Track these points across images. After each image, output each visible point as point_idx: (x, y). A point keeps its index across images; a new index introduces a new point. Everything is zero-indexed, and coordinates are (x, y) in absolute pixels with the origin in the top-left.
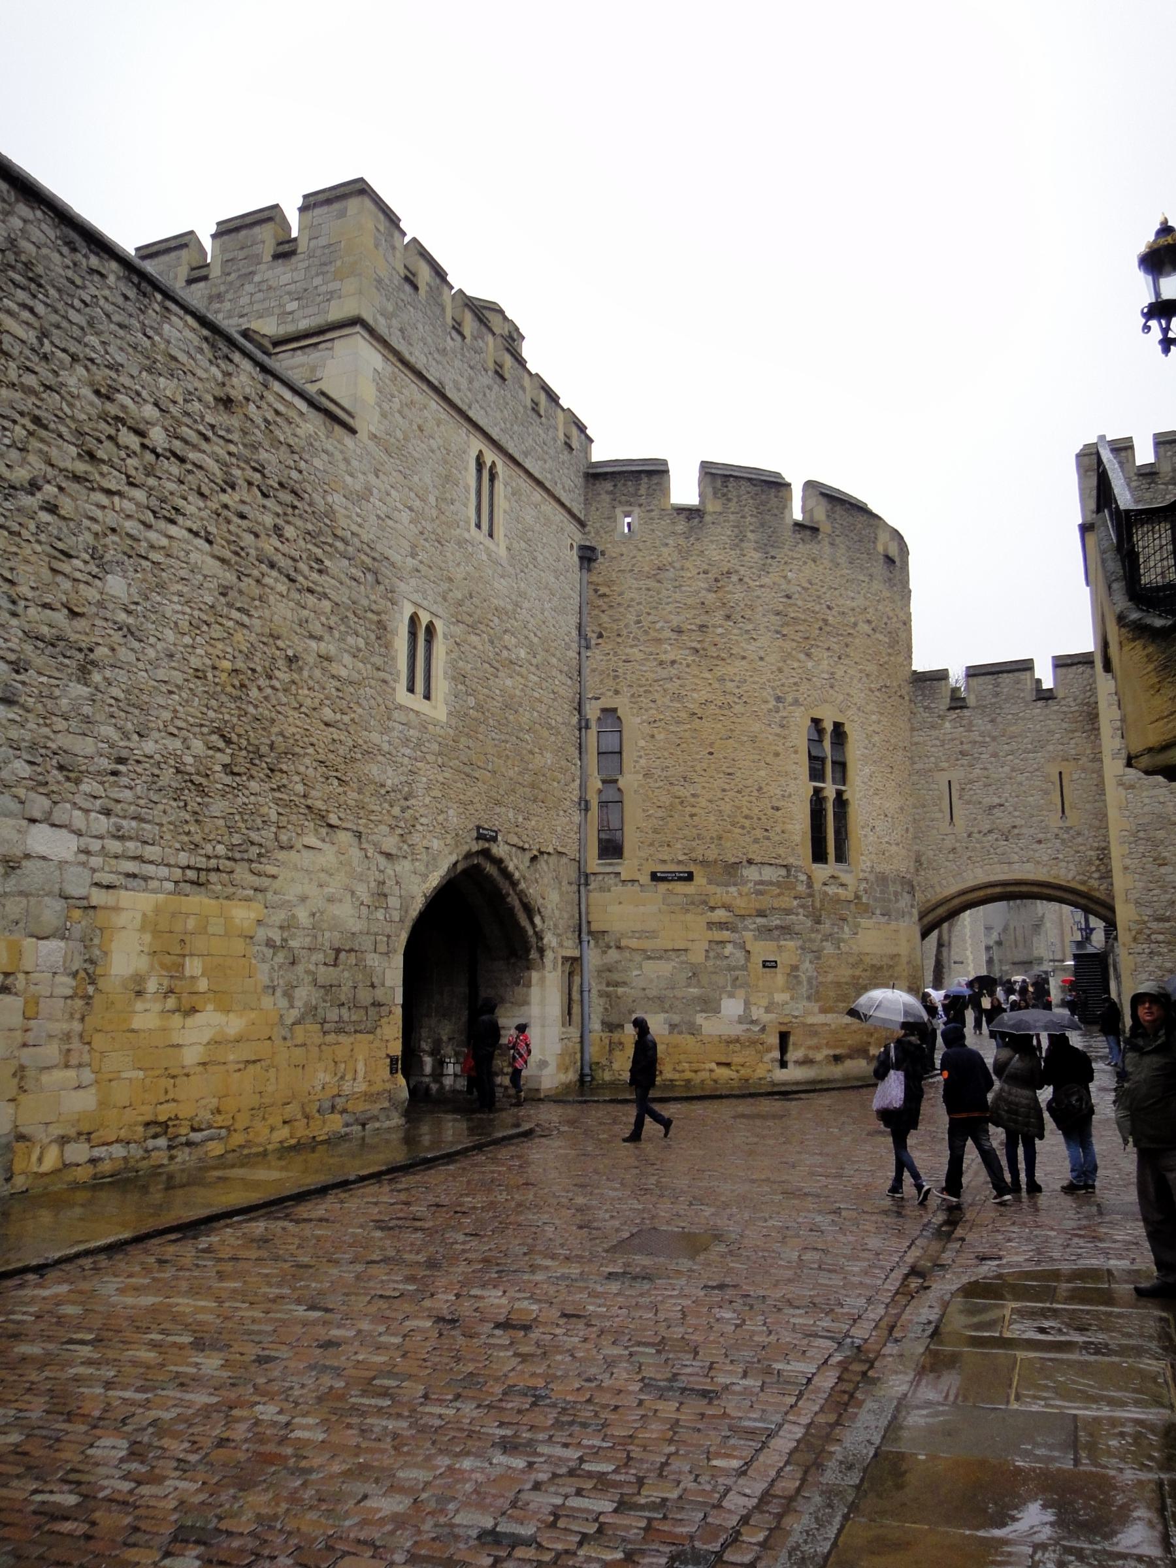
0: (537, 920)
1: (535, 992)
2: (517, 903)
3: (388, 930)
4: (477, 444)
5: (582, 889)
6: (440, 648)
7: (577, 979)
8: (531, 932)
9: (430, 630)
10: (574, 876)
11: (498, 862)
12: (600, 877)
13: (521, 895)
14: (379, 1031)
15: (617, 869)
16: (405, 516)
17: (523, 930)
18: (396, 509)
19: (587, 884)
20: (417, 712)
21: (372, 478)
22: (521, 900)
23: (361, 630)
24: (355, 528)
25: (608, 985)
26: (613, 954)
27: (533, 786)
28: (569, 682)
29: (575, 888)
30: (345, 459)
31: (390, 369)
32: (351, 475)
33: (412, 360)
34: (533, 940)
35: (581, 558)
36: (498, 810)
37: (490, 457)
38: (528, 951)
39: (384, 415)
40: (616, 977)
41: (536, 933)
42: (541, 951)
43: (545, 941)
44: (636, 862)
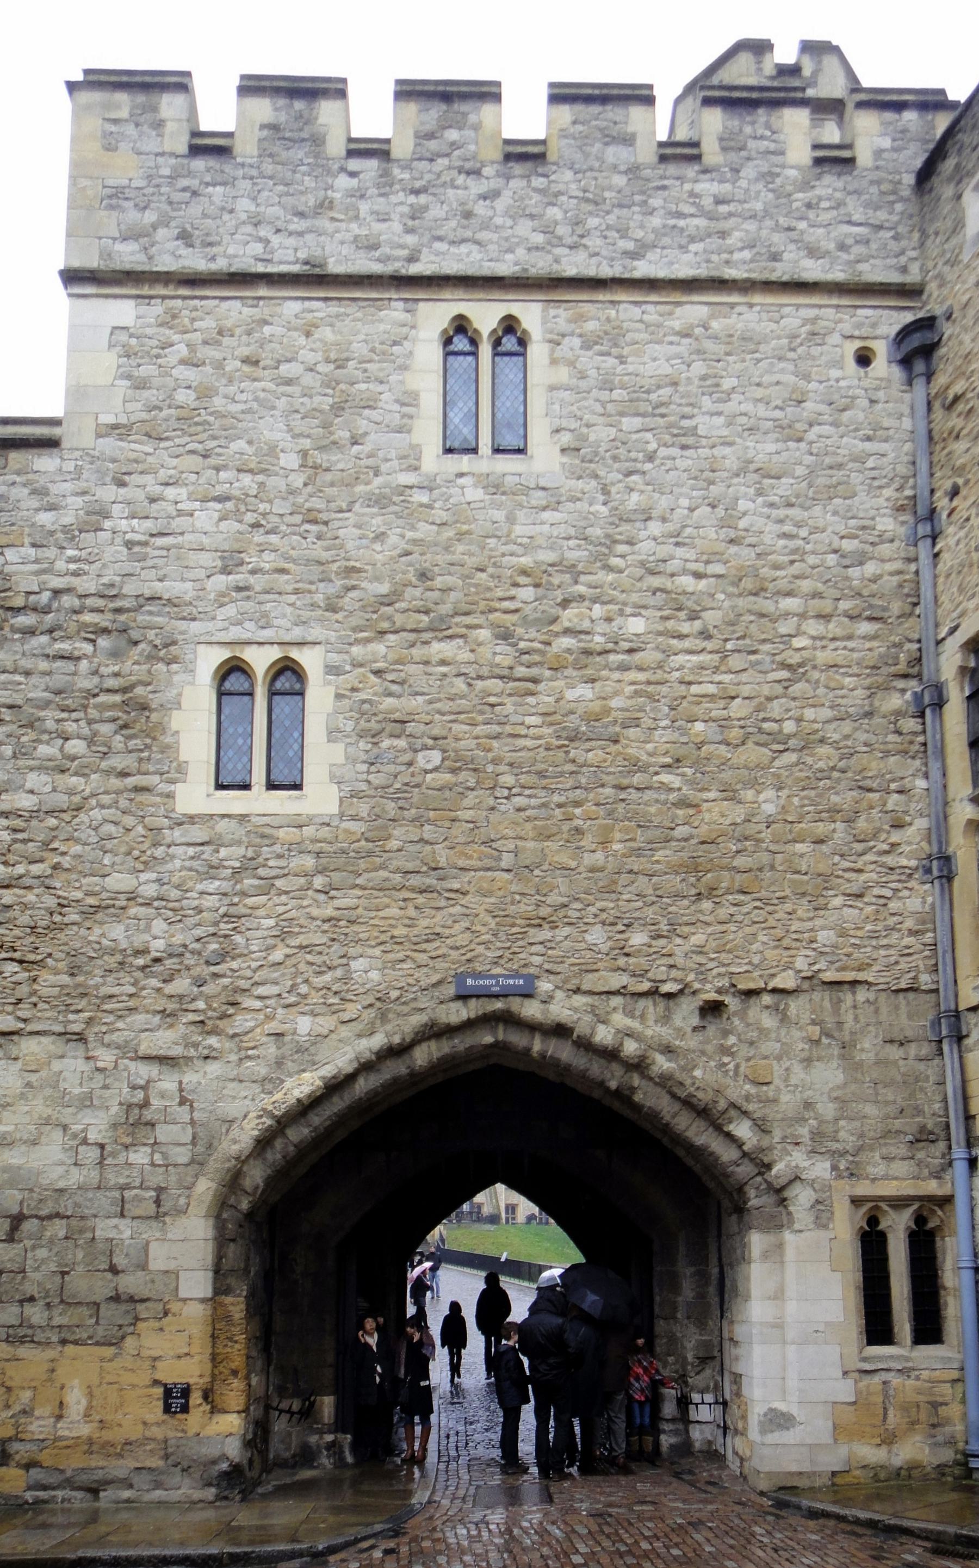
0: (742, 1130)
3: (157, 1179)
4: (437, 314)
6: (319, 698)
8: (727, 1154)
9: (288, 675)
11: (560, 1031)
14: (130, 1342)
16: (206, 517)
17: (699, 1153)
18: (180, 513)
19: (959, 1038)
20: (243, 818)
21: (108, 493)
22: (674, 1096)
23: (71, 727)
24: (57, 583)
27: (694, 867)
28: (865, 628)
30: (34, 492)
31: (157, 309)
32: (52, 508)
33: (221, 265)
35: (906, 362)
37: (485, 315)
39: (141, 385)
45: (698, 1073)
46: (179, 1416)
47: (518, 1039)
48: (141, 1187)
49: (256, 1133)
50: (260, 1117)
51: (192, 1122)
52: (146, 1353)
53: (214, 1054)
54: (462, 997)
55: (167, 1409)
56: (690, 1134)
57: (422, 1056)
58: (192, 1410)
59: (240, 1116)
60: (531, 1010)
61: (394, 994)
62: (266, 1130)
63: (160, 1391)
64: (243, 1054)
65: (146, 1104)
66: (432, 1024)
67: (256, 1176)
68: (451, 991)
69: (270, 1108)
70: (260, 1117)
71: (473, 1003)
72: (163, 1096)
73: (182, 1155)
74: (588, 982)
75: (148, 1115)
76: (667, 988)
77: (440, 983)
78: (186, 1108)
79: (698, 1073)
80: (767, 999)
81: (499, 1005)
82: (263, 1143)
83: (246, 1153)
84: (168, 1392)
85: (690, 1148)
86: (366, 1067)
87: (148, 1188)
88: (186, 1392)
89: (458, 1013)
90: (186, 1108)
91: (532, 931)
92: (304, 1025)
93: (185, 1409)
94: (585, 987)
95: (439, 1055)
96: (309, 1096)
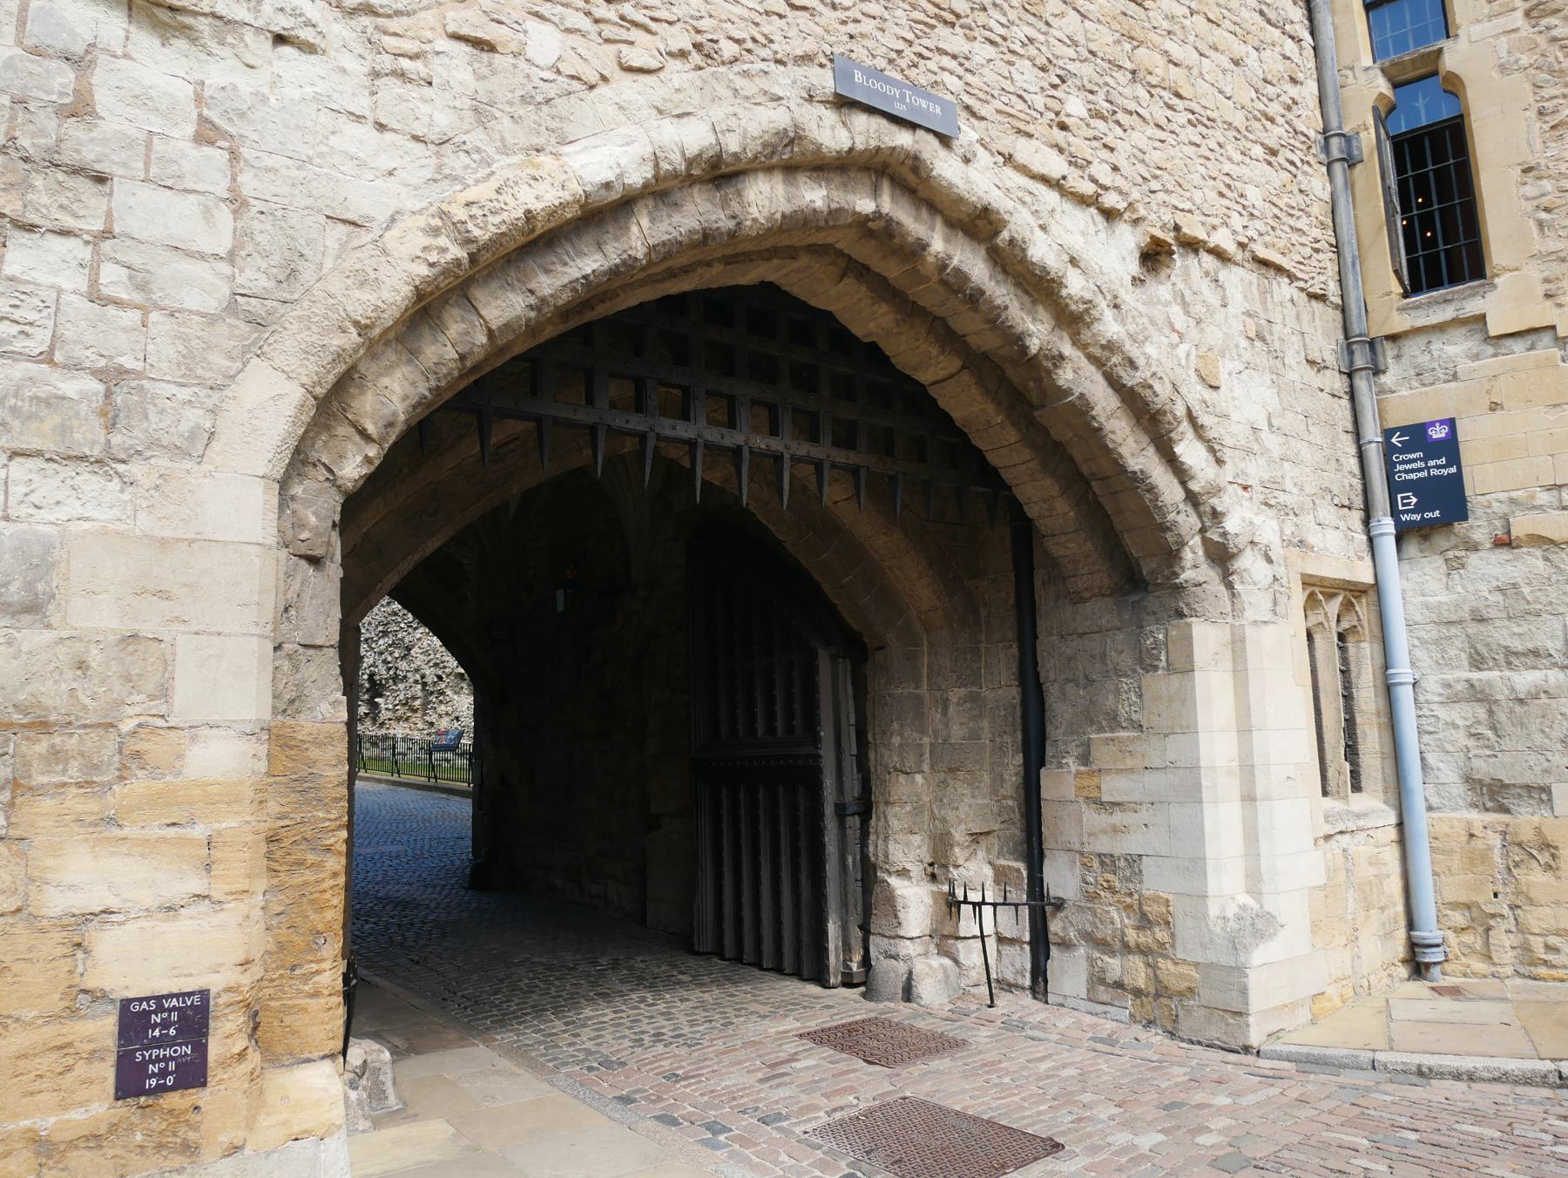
0: (1189, 451)
1: (1212, 686)
2: (1104, 402)
5: (1361, 383)
7: (1365, 653)
10: (1326, 344)
11: (979, 224)
12: (1412, 348)
13: (1105, 358)
15: (1473, 306)
17: (1137, 482)
25: (1477, 662)
26: (1489, 567)
29: (1339, 384)
34: (1187, 522)
36: (954, 41)
38: (1172, 556)
40: (1503, 634)
41: (1192, 498)
42: (1221, 556)
43: (1231, 524)
44: (1534, 273)
45: (1150, 349)
46: (175, 1100)
47: (912, 223)
48: (47, 358)
49: (424, 270)
50: (436, 232)
51: (237, 202)
52: (56, 903)
53: (306, 34)
54: (844, 103)
55: (130, 1083)
56: (1124, 451)
57: (765, 199)
58: (215, 1073)
59: (382, 217)
60: (946, 168)
61: (729, 49)
62: (446, 272)
63: (105, 1027)
64: (387, 62)
65: (80, 109)
66: (792, 138)
67: (393, 395)
68: (825, 81)
69: (460, 214)
70: (436, 232)
71: (861, 120)
72: (142, 99)
73: (202, 289)
74: (1025, 151)
75: (85, 145)
76: (1111, 200)
77: (806, 58)
78: (218, 156)
79: (1150, 349)
80: (1208, 260)
81: (903, 139)
82: (426, 309)
83: (388, 319)
84: (135, 1021)
85: (1119, 468)
86: (662, 190)
87: (77, 367)
88: (193, 1017)
89: (833, 134)
90: (218, 156)
91: (942, 30)
92: (544, 43)
93: (193, 1074)
94: (1020, 157)
95: (787, 208)
96: (552, 212)
